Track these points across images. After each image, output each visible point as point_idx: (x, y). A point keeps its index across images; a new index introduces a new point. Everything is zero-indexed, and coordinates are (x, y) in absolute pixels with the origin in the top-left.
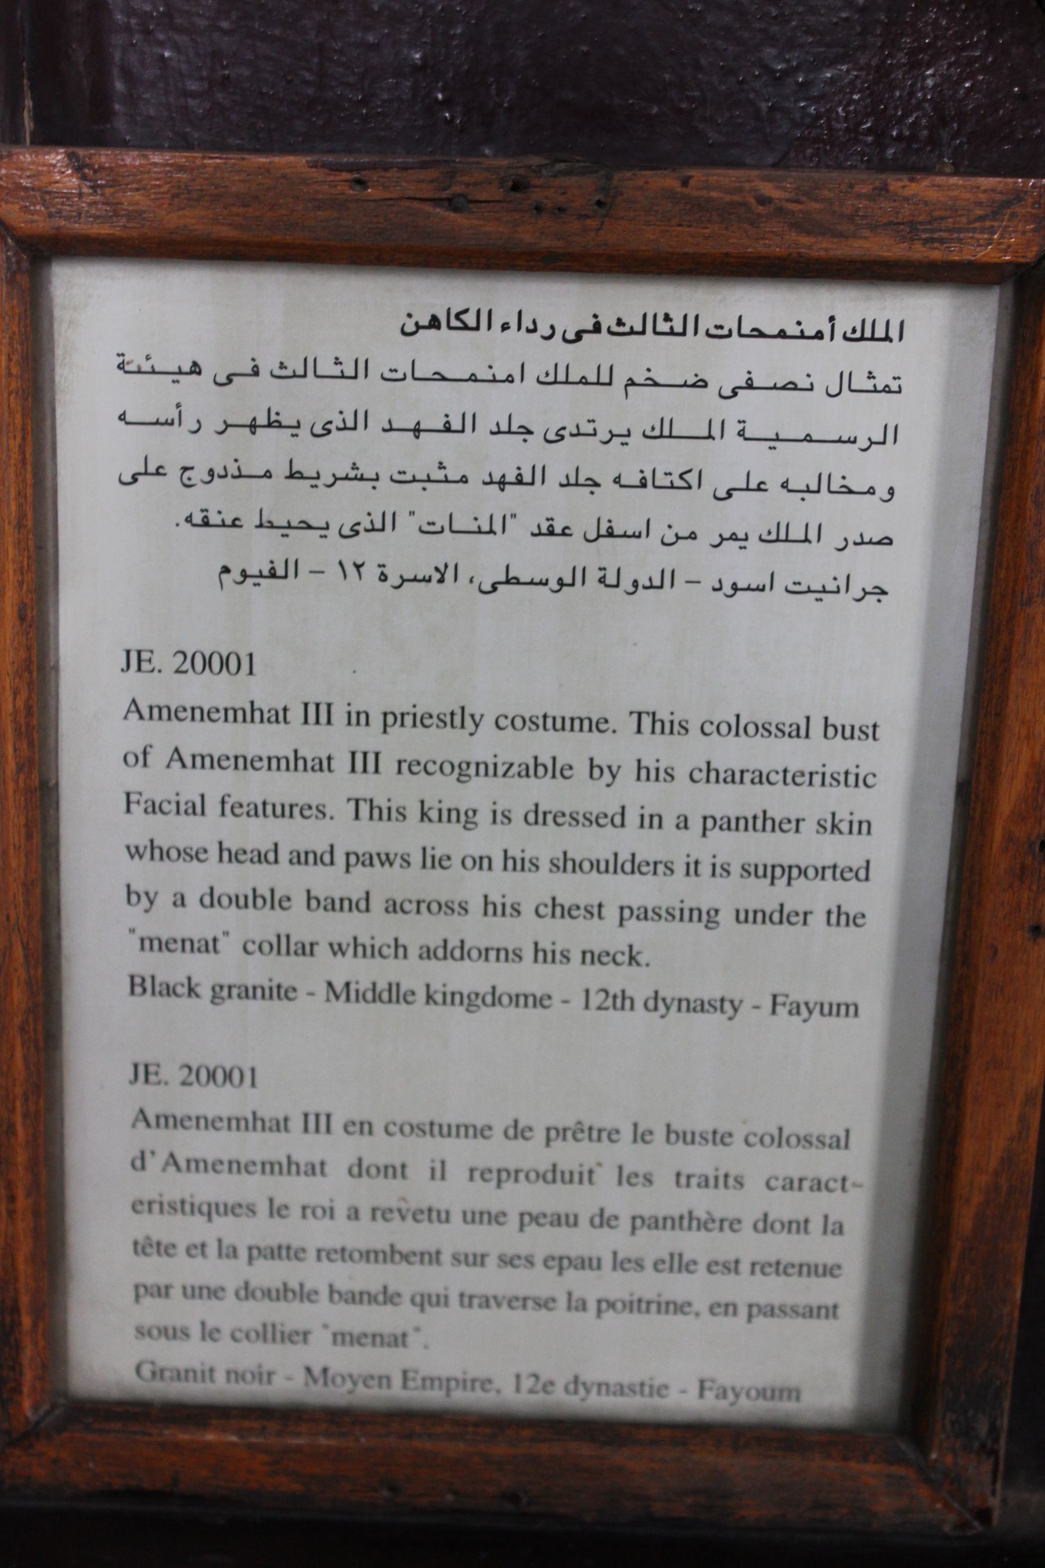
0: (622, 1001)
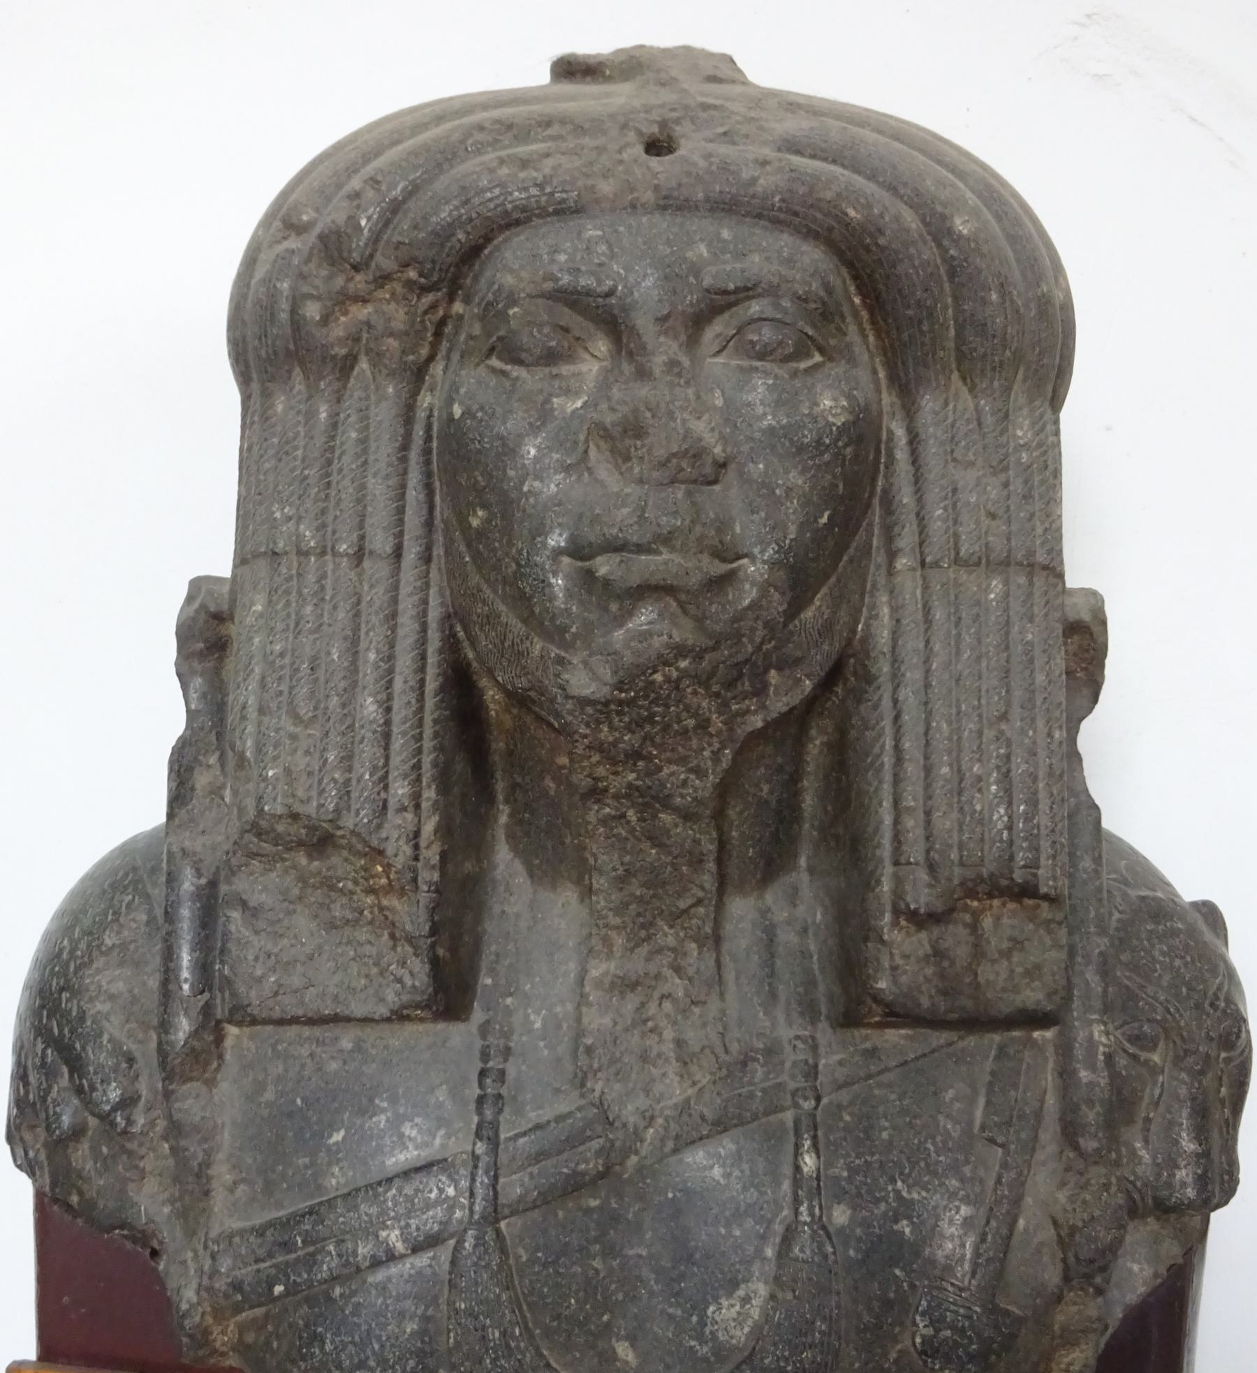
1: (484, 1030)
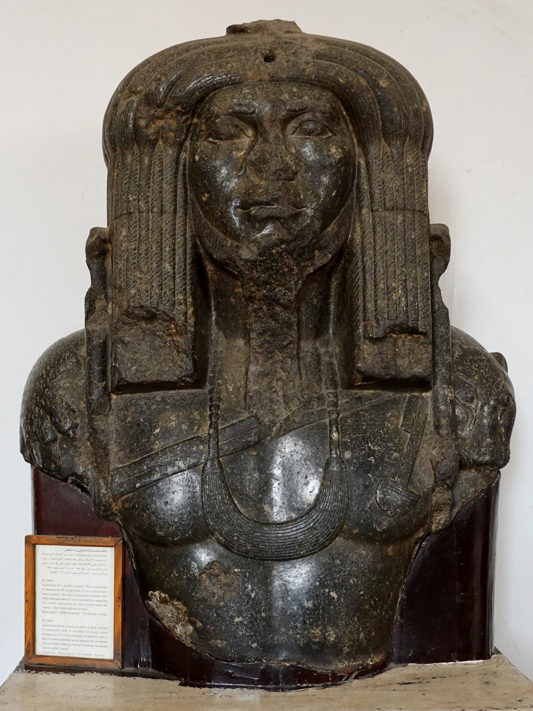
0: (86, 614)
1: (211, 391)
